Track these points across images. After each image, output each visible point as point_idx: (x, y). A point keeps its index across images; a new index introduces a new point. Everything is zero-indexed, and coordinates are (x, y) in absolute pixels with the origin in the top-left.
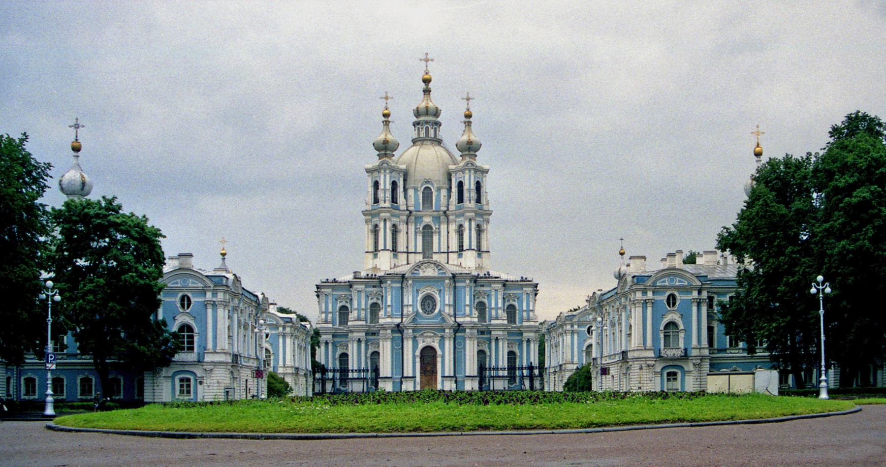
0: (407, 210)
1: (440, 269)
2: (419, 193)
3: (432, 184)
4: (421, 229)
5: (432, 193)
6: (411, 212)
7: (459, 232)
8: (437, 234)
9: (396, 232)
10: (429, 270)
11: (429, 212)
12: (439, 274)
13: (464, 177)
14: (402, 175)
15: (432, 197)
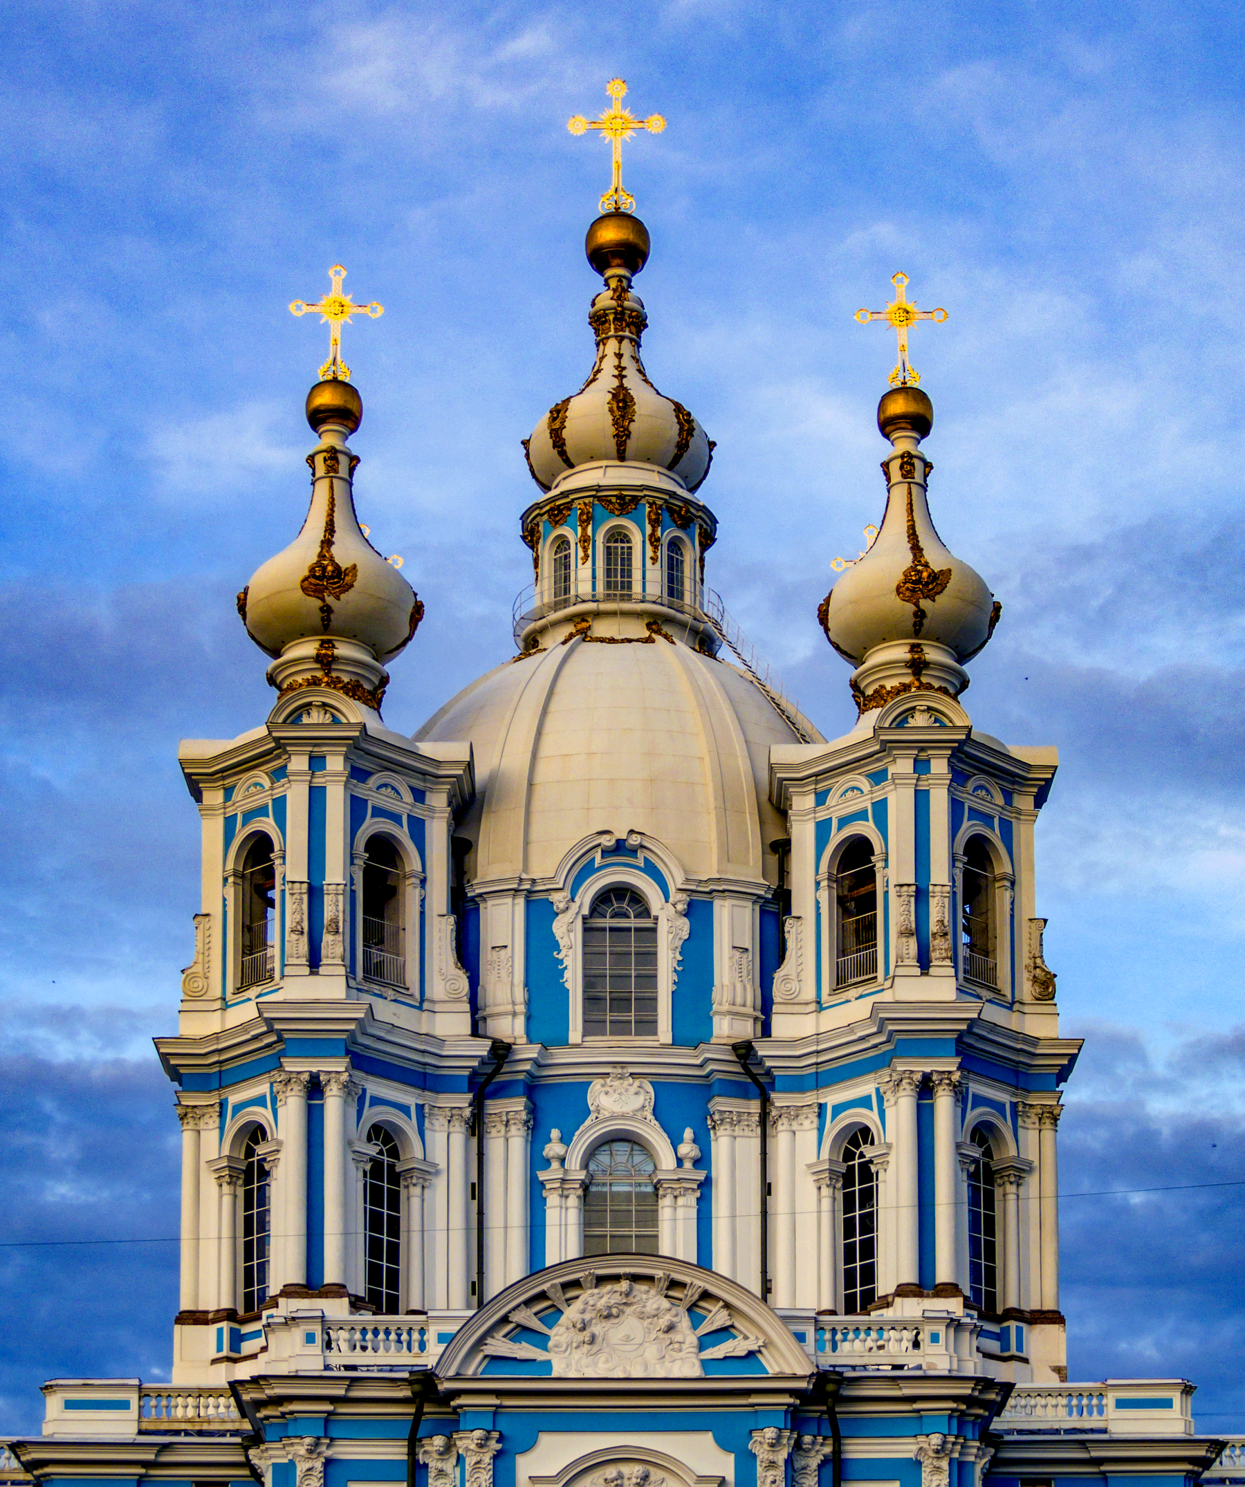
0: (475, 1033)
1: (725, 1332)
2: (559, 927)
3: (651, 870)
4: (574, 1162)
5: (651, 932)
6: (501, 1051)
7: (848, 1179)
8: (691, 1199)
9: (395, 1178)
10: (630, 1325)
11: (629, 1048)
12: (704, 1363)
13: (880, 809)
14: (439, 800)
15: (649, 957)
